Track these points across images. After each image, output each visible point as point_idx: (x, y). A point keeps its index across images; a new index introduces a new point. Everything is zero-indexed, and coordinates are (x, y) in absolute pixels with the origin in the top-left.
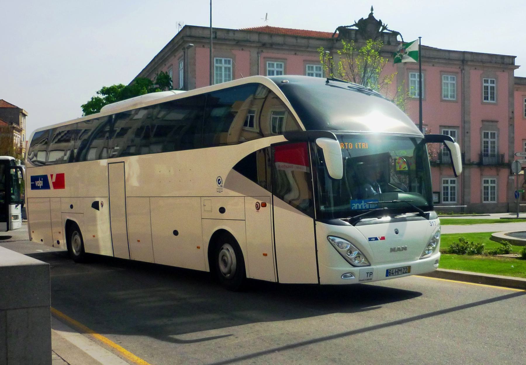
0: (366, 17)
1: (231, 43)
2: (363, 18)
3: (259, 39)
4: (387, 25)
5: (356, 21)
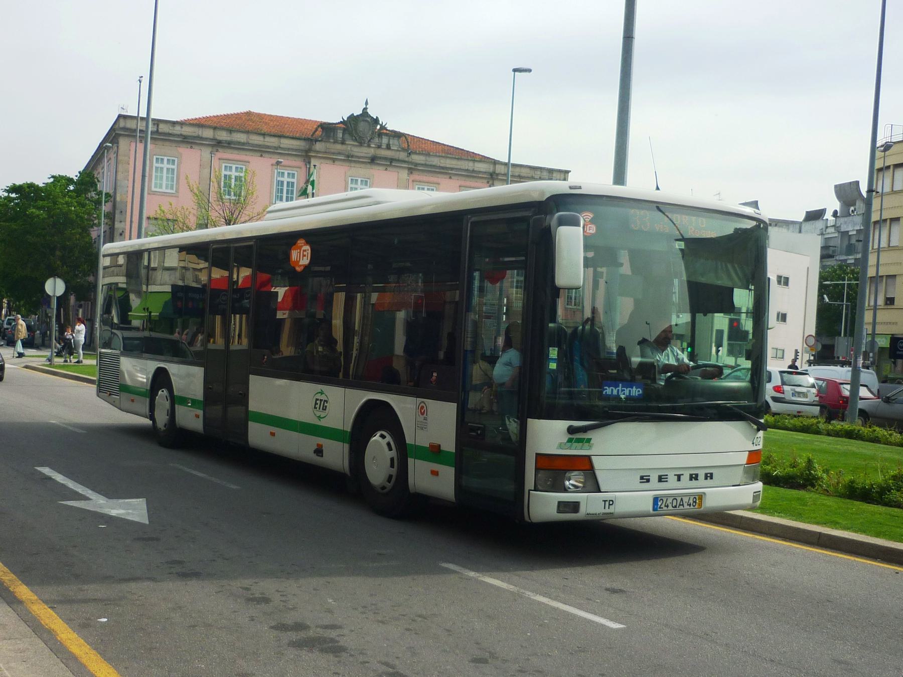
0: (358, 112)
2: (353, 114)
3: (214, 135)
4: (386, 124)
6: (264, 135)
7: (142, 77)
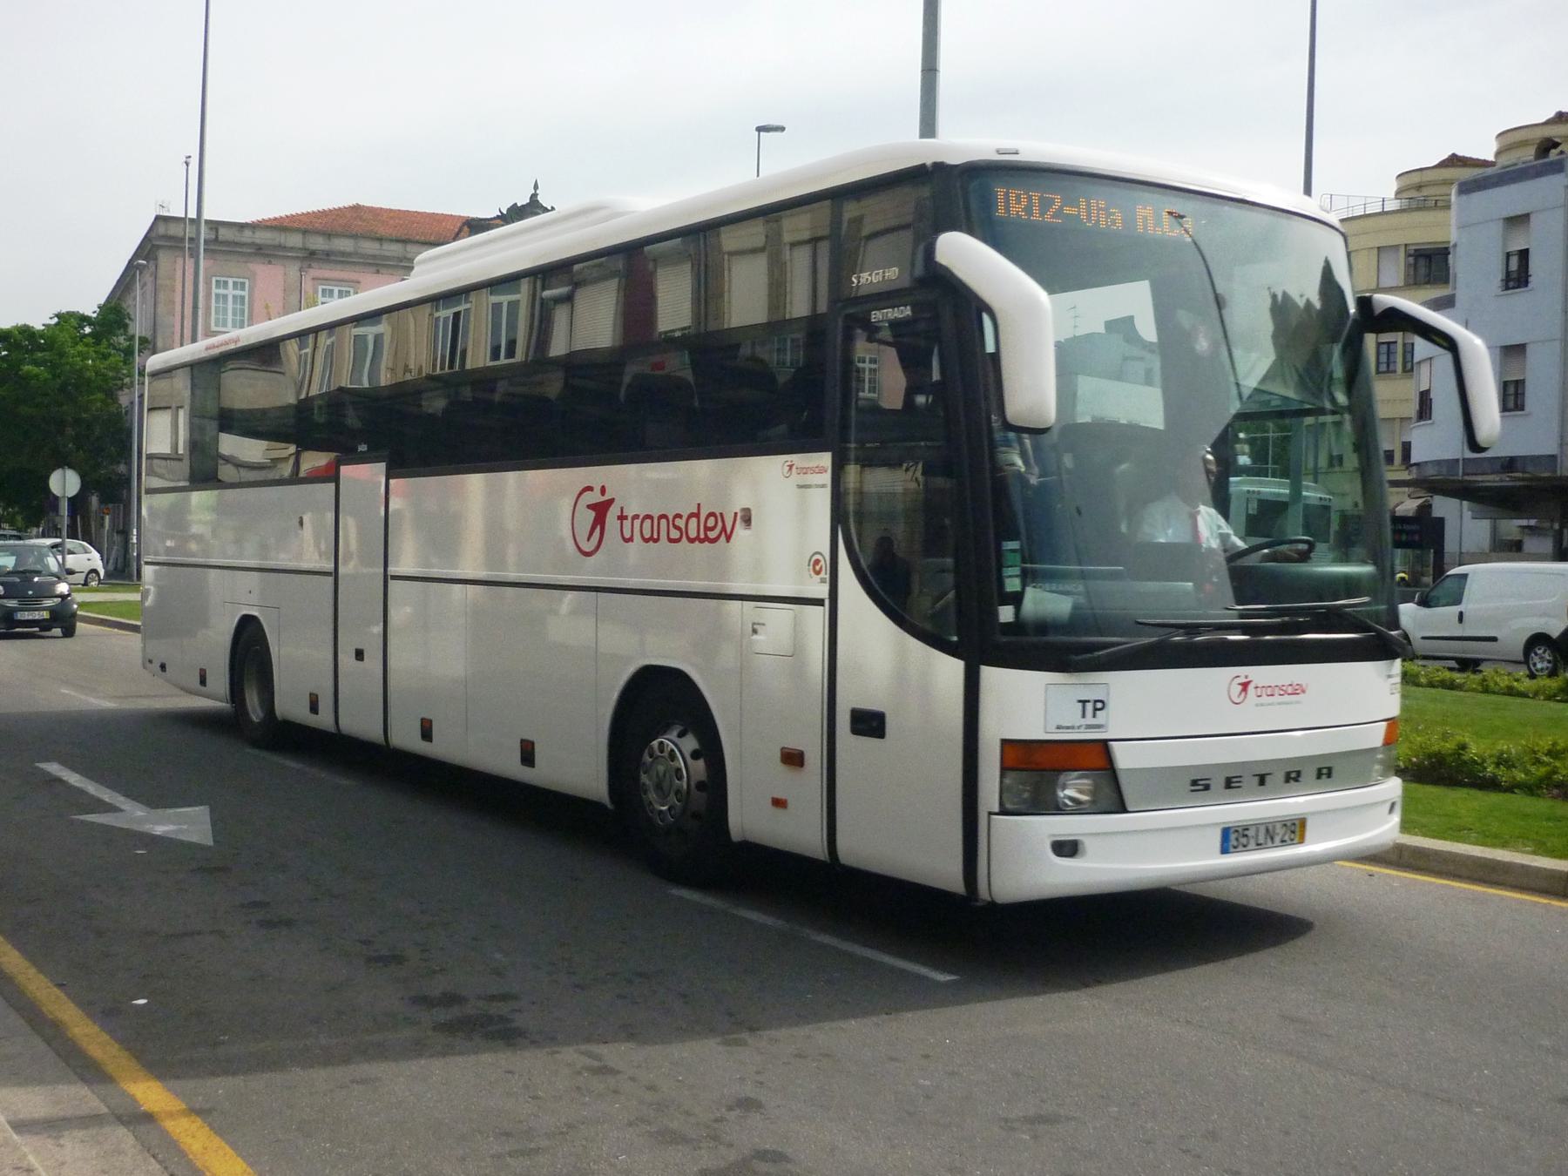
1: (244, 250)
2: (516, 204)
3: (304, 243)
5: (502, 210)
6: (380, 240)
7: (190, 157)
